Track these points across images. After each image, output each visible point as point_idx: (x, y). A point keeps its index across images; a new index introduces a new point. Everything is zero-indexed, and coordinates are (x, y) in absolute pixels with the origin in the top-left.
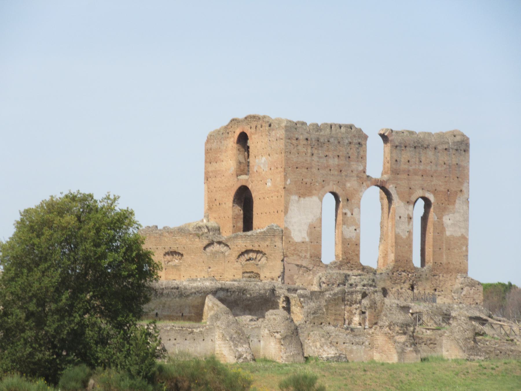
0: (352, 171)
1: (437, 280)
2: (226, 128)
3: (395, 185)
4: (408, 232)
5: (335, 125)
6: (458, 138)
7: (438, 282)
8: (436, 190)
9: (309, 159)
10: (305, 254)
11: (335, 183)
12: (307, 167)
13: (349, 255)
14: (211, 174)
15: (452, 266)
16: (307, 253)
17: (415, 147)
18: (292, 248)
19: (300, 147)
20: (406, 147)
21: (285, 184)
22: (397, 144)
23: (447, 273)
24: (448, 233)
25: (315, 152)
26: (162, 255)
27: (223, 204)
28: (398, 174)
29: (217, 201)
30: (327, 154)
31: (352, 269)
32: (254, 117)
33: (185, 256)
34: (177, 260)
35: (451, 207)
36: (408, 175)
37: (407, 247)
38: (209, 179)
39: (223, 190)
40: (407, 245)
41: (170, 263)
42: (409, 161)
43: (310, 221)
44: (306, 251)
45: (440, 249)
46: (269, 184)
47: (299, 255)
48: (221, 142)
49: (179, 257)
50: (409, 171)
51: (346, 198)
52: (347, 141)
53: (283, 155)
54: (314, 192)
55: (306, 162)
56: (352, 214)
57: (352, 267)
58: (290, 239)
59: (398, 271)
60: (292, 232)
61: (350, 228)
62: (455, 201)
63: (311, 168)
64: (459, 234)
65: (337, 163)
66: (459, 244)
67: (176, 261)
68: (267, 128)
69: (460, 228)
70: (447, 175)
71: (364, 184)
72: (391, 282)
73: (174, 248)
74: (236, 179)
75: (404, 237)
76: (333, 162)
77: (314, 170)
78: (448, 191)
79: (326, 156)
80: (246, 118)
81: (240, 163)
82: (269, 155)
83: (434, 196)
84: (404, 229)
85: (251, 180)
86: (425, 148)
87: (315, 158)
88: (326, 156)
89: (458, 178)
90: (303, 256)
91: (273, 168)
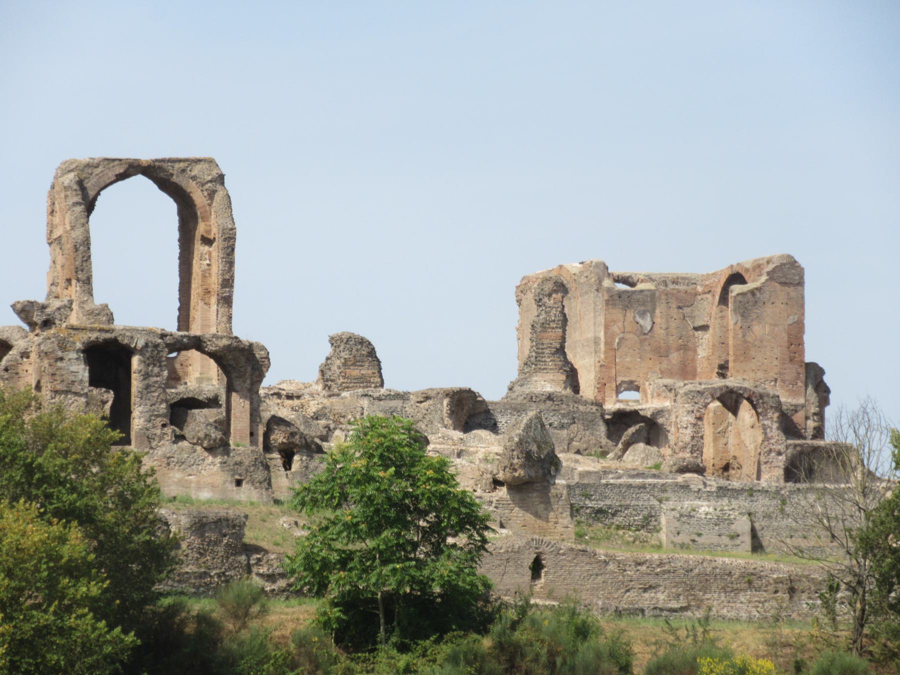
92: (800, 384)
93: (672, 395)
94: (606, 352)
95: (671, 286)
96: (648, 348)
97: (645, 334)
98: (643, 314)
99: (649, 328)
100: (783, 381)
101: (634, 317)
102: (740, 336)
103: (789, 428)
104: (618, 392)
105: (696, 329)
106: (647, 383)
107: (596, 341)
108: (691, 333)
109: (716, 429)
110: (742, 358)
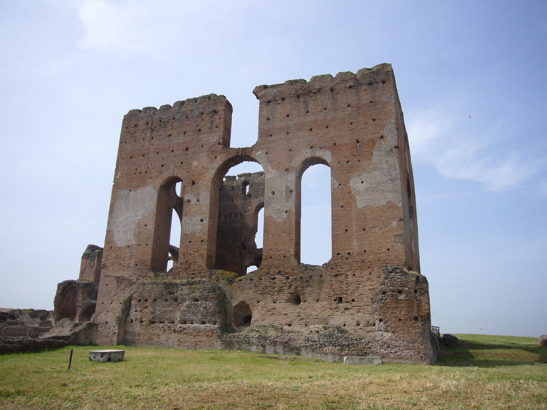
0: (202, 146)
1: (342, 283)
3: (265, 151)
4: (286, 212)
7: (344, 286)
8: (335, 144)
9: (146, 143)
10: (129, 262)
11: (176, 165)
12: (142, 154)
13: (189, 257)
15: (371, 256)
16: (131, 260)
18: (113, 256)
20: (283, 99)
22: (270, 98)
23: (361, 269)
24: (360, 205)
28: (271, 136)
30: (170, 133)
31: (194, 276)
35: (364, 163)
36: (288, 133)
37: (284, 235)
40: (284, 232)
42: (288, 116)
43: (140, 218)
44: (131, 258)
45: (347, 231)
47: (121, 264)
50: (288, 127)
51: (191, 181)
52: (197, 112)
55: (143, 148)
56: (198, 201)
57: (193, 274)
58: (112, 245)
59: (269, 273)
60: (116, 235)
61: (194, 219)
62: (372, 154)
63: (148, 153)
64: (384, 202)
65: (181, 141)
66: (383, 218)
69: (383, 192)
70: (355, 120)
71: (218, 158)
72: (256, 292)
75: (280, 220)
78: (358, 141)
79: (170, 135)
83: (333, 154)
84: (279, 209)
86: (315, 93)
87: (155, 141)
88: (170, 135)
89: (374, 120)
90: (126, 264)
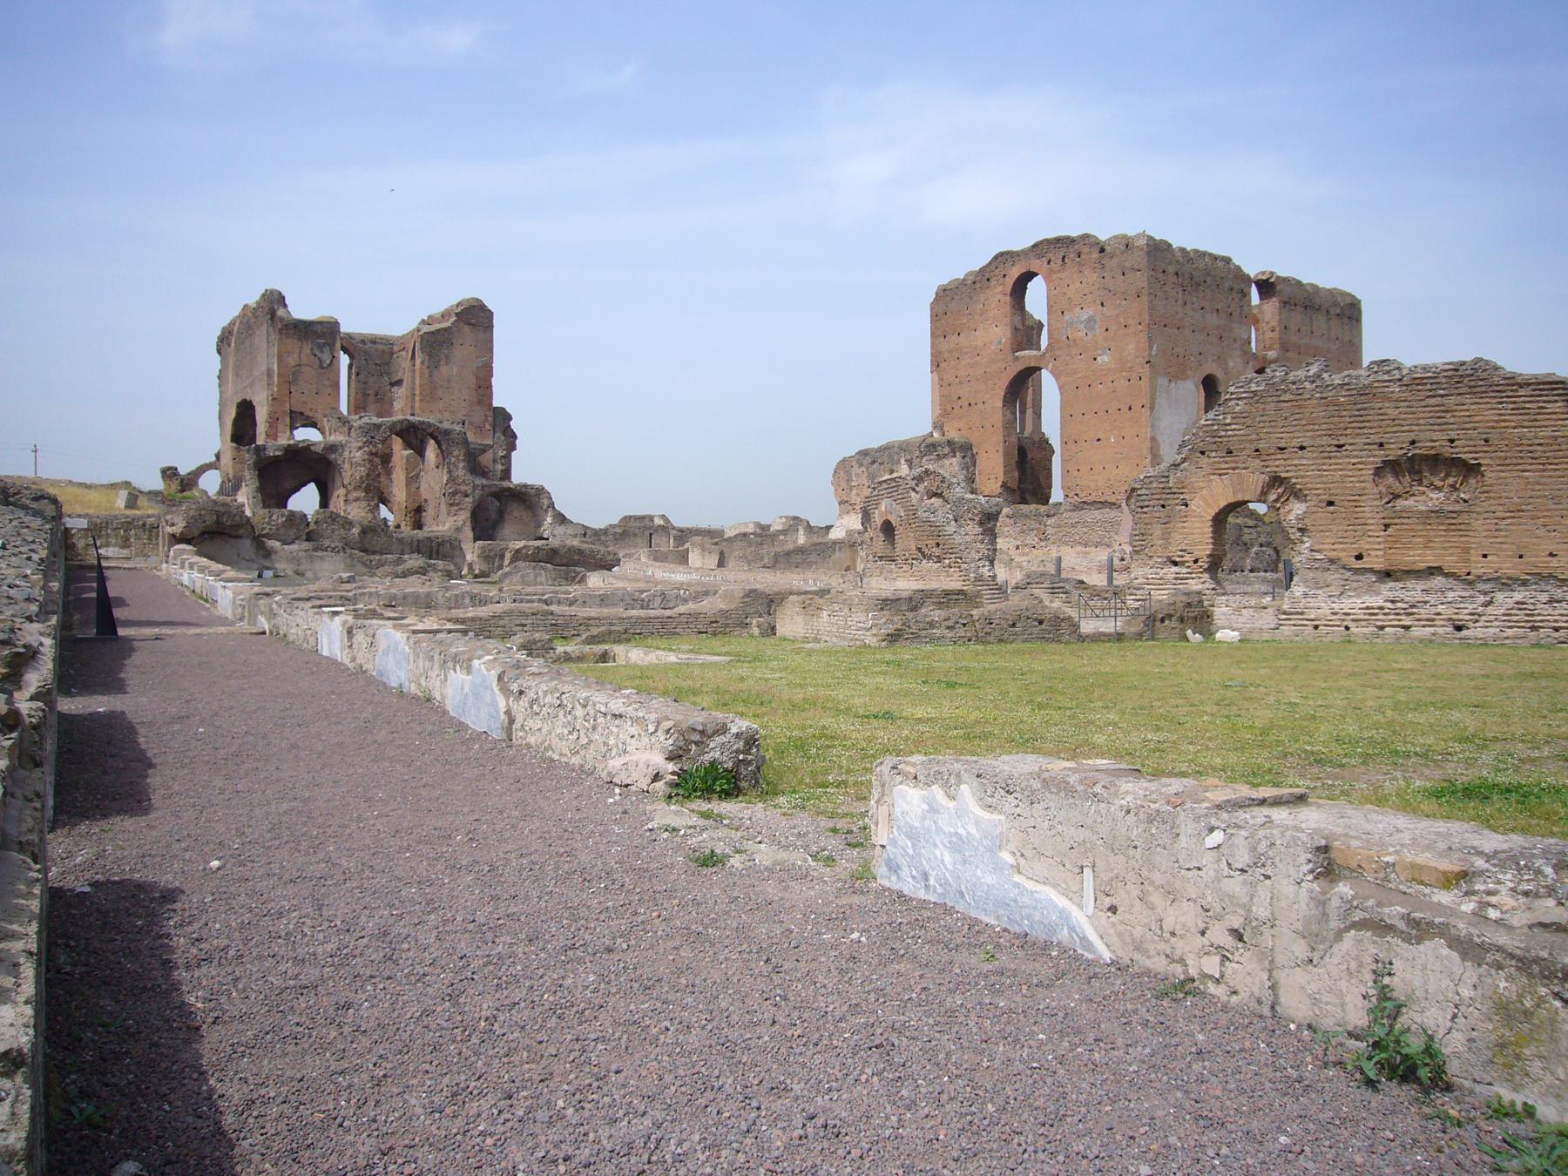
2: (982, 270)
5: (1210, 254)
6: (1349, 300)
14: (946, 355)
17: (1306, 307)
19: (1167, 288)
21: (1150, 355)
22: (1286, 299)
25: (1188, 298)
26: (1368, 473)
27: (980, 405)
29: (963, 399)
32: (1058, 240)
33: (1490, 476)
34: (1439, 489)
38: (943, 365)
39: (978, 380)
41: (1400, 503)
46: (1104, 359)
48: (971, 298)
49: (1451, 480)
53: (1145, 299)
54: (1189, 372)
67: (1434, 495)
68: (1095, 255)
73: (1434, 440)
74: (1010, 357)
76: (1213, 320)
77: (1187, 332)
79: (1202, 308)
80: (1035, 246)
81: (1016, 329)
82: (1102, 305)
85: (1051, 356)
91: (1113, 328)
92: (488, 427)
93: (346, 429)
94: (279, 385)
95: (370, 345)
96: (327, 383)
97: (323, 368)
98: (321, 347)
99: (328, 362)
100: (471, 423)
101: (312, 349)
102: (427, 376)
103: (476, 468)
104: (293, 428)
105: (392, 384)
106: (325, 420)
107: (269, 373)
108: (388, 388)
109: (408, 473)
110: (429, 399)
